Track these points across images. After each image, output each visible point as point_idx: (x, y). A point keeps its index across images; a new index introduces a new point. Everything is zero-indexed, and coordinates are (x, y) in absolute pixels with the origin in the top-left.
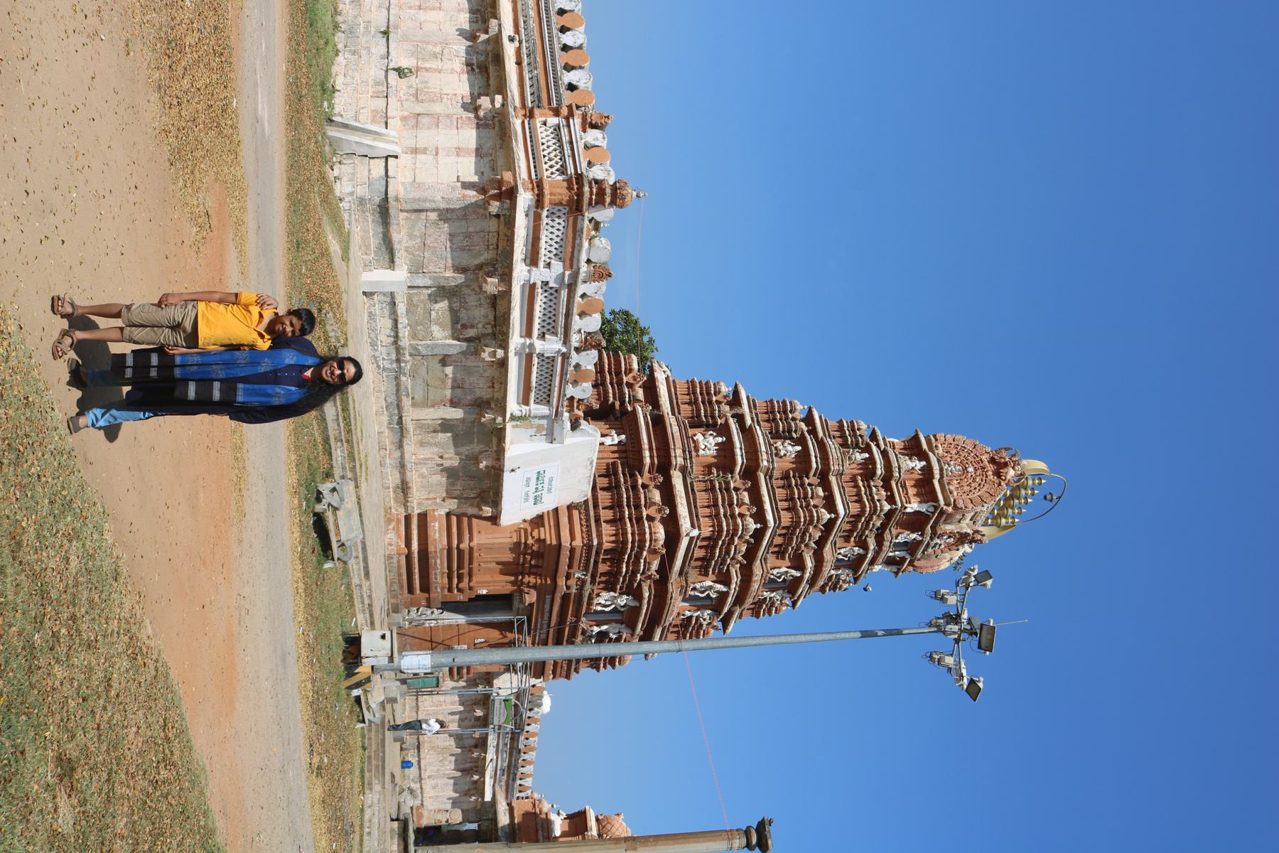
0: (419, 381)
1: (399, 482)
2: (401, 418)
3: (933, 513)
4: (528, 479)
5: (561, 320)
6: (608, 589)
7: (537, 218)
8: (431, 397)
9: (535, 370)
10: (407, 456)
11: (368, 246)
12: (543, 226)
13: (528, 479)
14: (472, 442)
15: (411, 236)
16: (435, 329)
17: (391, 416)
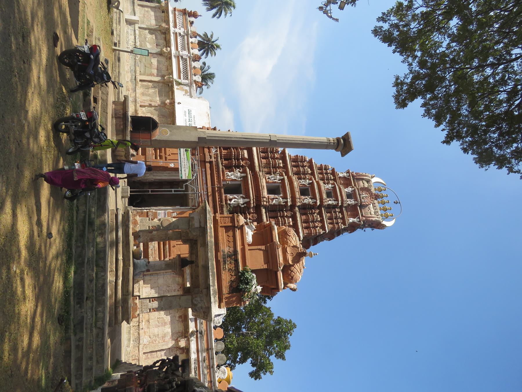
0: (142, 64)
1: (133, 111)
2: (135, 77)
3: (349, 176)
4: (185, 112)
5: (186, 45)
6: (230, 172)
7: (175, 15)
8: (147, 72)
9: (181, 64)
10: (137, 95)
11: (128, 11)
12: (177, 19)
13: (185, 112)
14: (162, 96)
15: (140, 14)
16: (148, 44)
17: (132, 77)
